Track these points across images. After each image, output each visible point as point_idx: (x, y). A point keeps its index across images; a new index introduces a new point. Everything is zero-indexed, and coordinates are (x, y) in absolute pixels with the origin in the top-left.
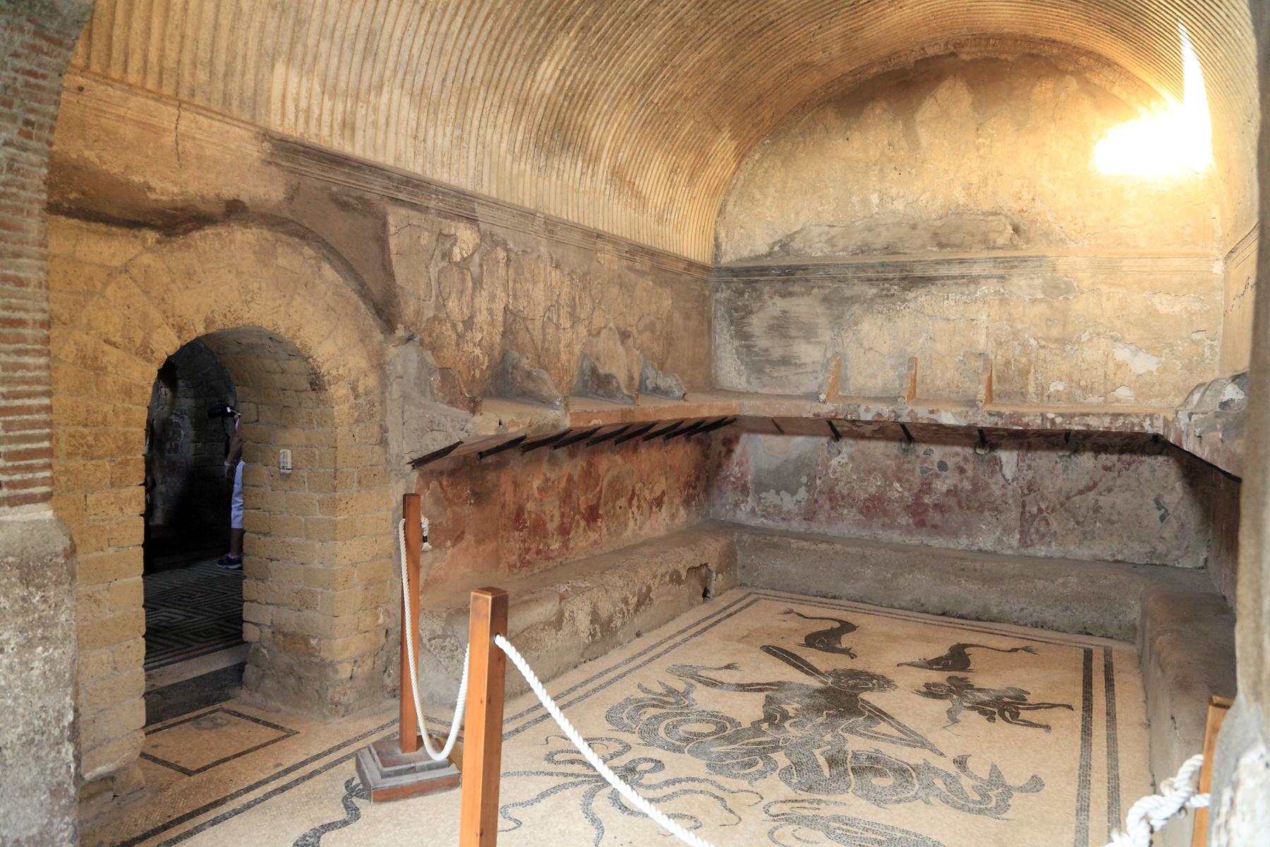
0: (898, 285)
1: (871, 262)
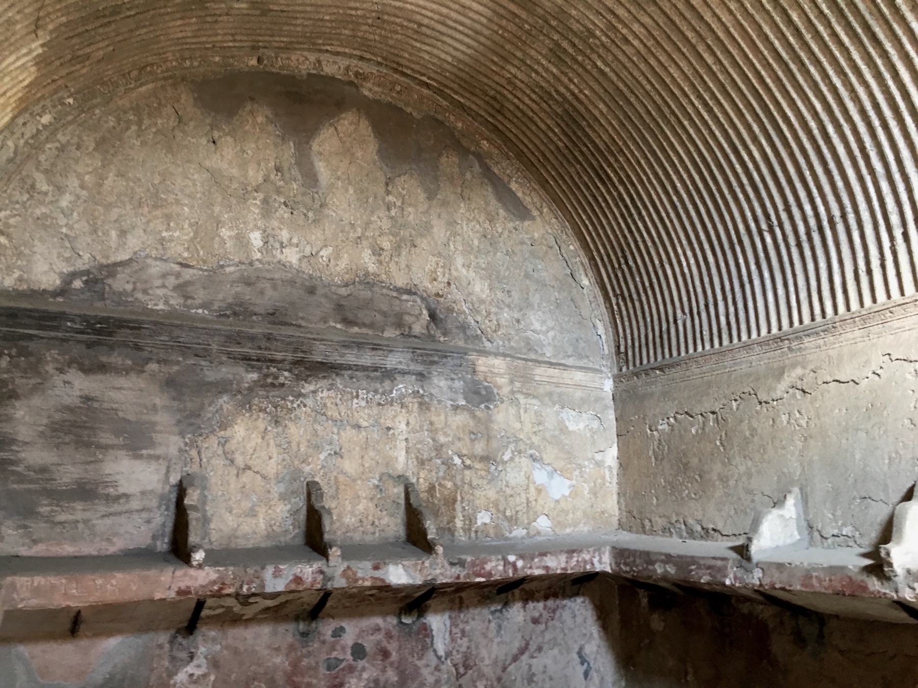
0: (290, 371)
1: (254, 331)
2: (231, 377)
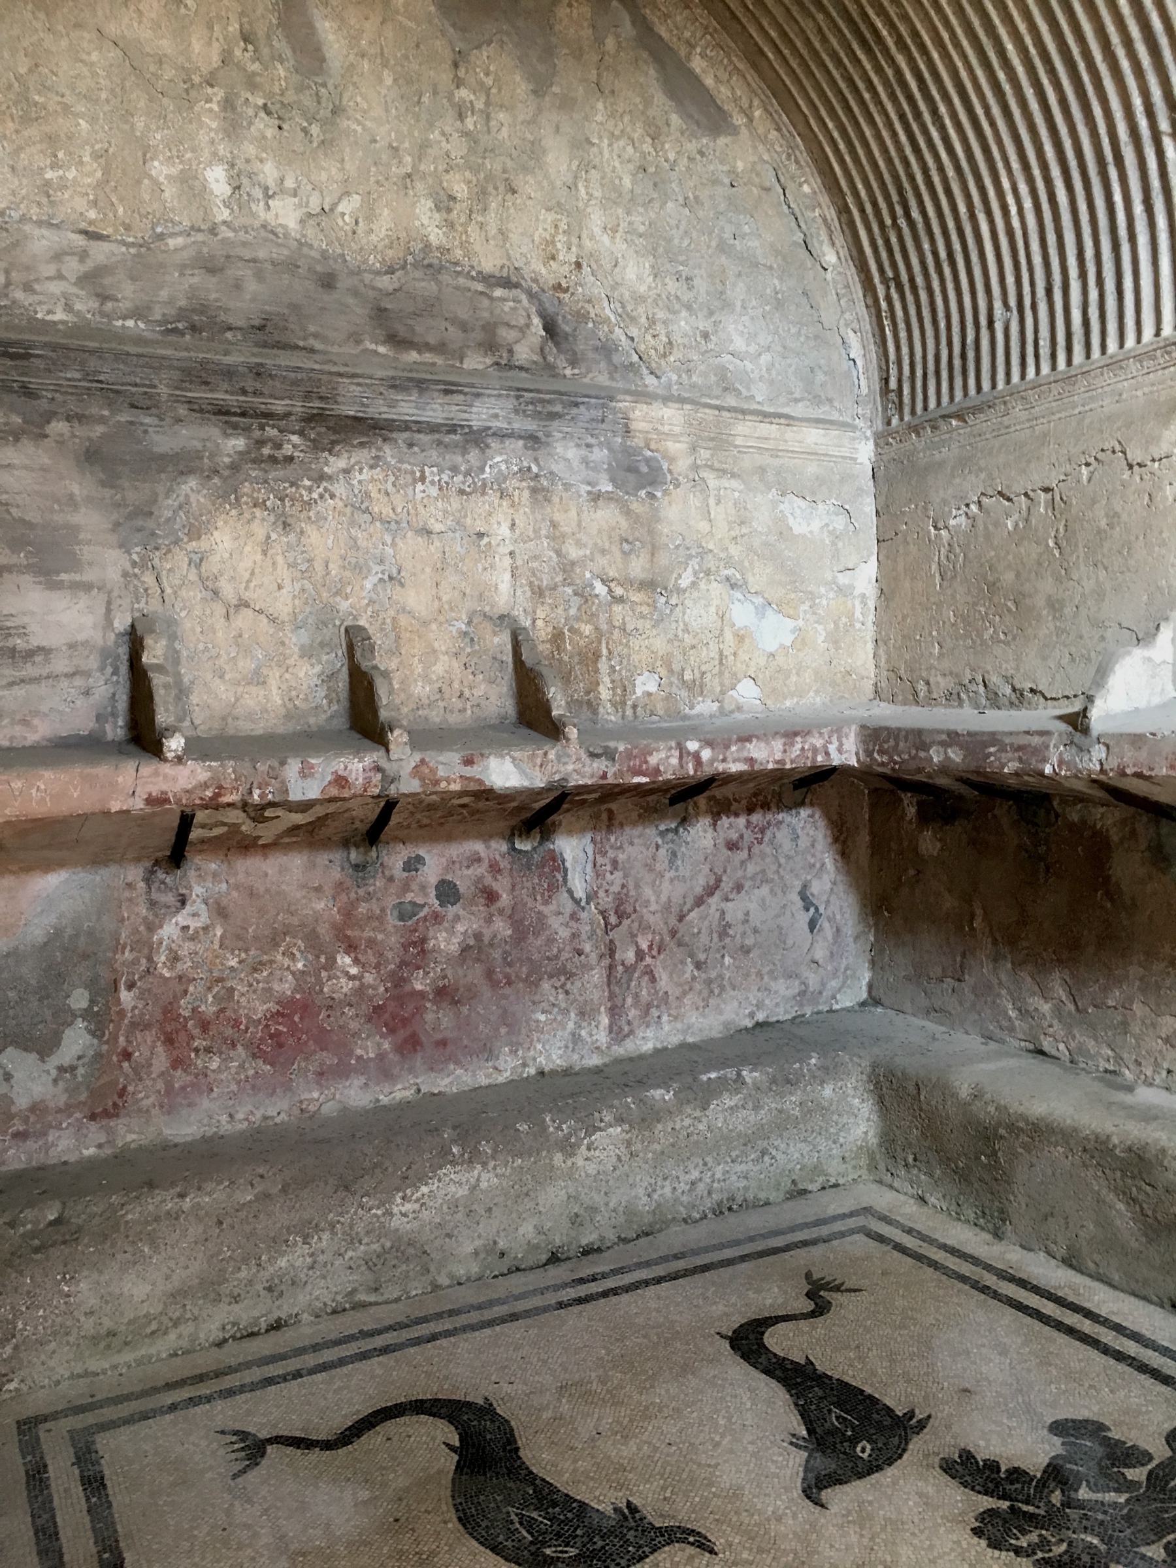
0: (301, 433)
1: (228, 360)
2: (198, 445)
